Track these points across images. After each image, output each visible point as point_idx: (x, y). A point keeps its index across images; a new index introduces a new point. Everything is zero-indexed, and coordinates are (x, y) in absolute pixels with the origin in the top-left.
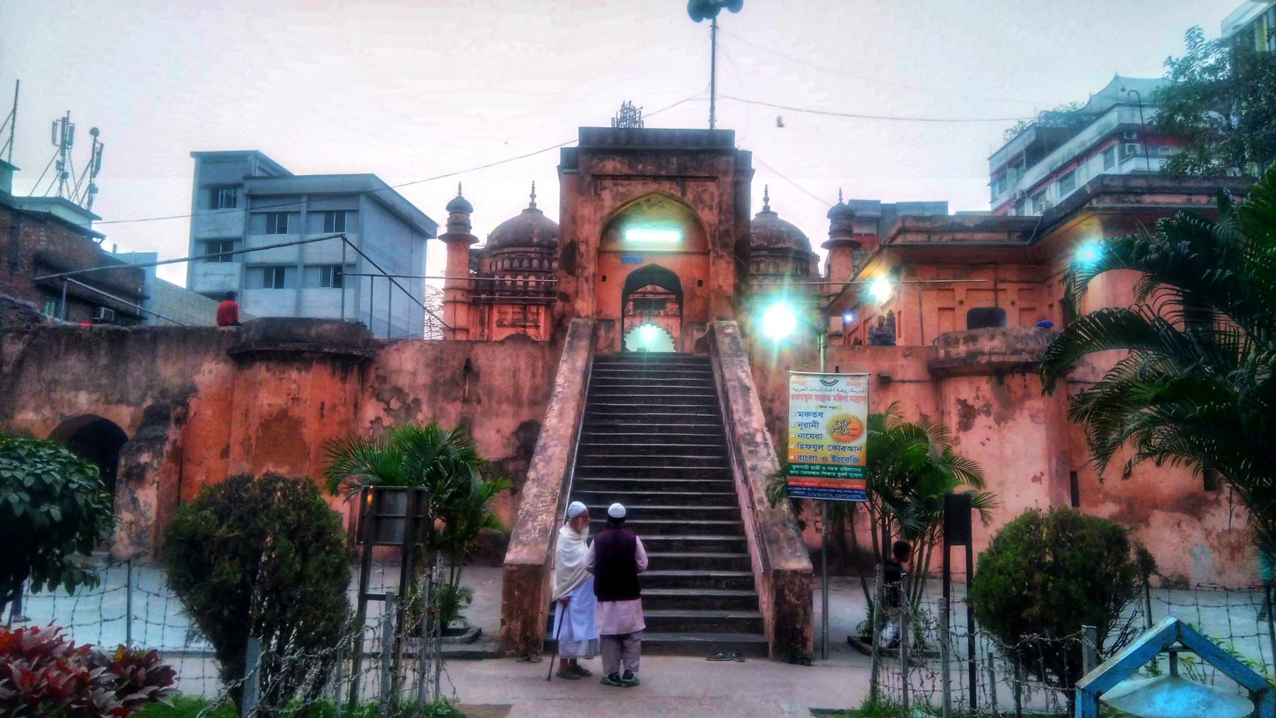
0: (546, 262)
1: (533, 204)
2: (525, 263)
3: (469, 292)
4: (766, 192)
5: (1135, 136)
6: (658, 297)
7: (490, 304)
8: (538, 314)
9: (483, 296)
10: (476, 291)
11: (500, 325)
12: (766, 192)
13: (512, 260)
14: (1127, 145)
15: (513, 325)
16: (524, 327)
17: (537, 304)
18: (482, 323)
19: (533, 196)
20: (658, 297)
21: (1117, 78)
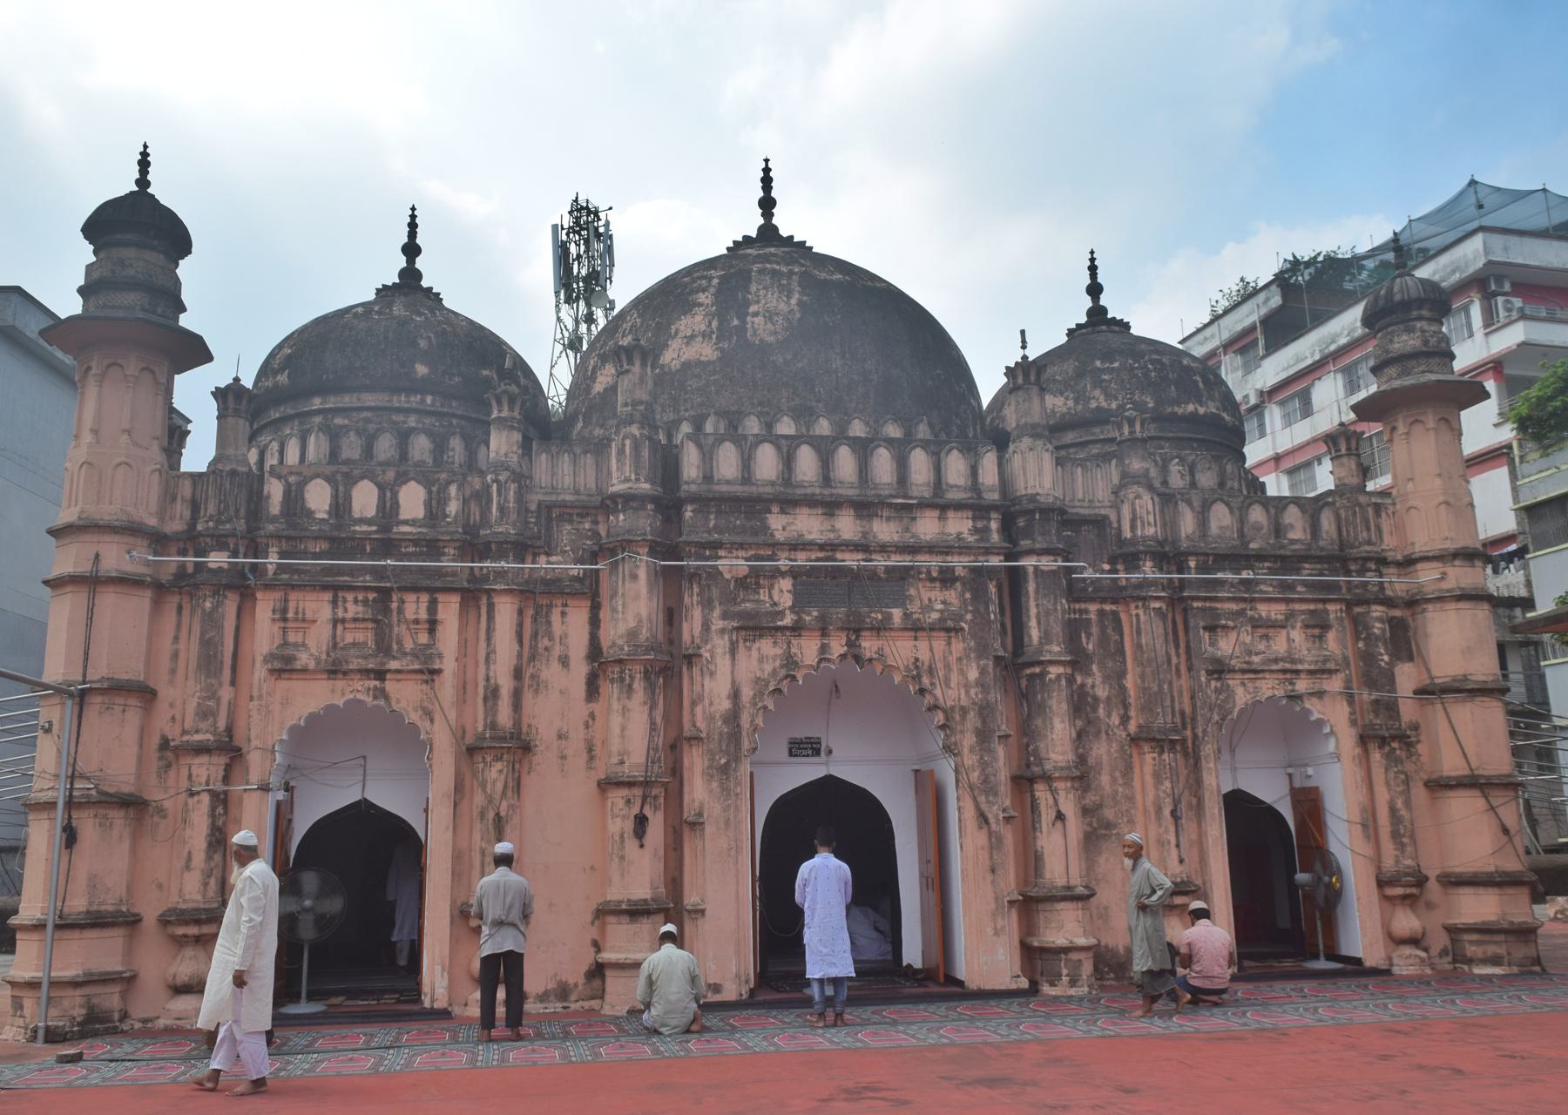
0: (456, 444)
1: (410, 275)
2: (385, 447)
3: (159, 541)
4: (1093, 269)
5: (1507, 287)
6: (880, 562)
7: (242, 585)
8: (432, 625)
9: (218, 559)
10: (191, 540)
11: (284, 666)
12: (1093, 269)
13: (334, 436)
14: (1500, 300)
15: (335, 671)
16: (380, 675)
17: (433, 586)
18: (209, 661)
19: (411, 250)
20: (880, 562)
21: (1473, 183)
